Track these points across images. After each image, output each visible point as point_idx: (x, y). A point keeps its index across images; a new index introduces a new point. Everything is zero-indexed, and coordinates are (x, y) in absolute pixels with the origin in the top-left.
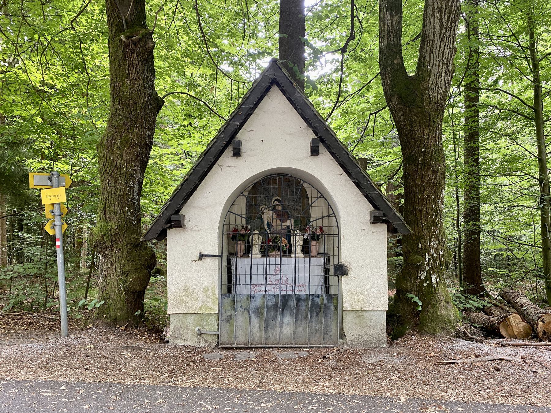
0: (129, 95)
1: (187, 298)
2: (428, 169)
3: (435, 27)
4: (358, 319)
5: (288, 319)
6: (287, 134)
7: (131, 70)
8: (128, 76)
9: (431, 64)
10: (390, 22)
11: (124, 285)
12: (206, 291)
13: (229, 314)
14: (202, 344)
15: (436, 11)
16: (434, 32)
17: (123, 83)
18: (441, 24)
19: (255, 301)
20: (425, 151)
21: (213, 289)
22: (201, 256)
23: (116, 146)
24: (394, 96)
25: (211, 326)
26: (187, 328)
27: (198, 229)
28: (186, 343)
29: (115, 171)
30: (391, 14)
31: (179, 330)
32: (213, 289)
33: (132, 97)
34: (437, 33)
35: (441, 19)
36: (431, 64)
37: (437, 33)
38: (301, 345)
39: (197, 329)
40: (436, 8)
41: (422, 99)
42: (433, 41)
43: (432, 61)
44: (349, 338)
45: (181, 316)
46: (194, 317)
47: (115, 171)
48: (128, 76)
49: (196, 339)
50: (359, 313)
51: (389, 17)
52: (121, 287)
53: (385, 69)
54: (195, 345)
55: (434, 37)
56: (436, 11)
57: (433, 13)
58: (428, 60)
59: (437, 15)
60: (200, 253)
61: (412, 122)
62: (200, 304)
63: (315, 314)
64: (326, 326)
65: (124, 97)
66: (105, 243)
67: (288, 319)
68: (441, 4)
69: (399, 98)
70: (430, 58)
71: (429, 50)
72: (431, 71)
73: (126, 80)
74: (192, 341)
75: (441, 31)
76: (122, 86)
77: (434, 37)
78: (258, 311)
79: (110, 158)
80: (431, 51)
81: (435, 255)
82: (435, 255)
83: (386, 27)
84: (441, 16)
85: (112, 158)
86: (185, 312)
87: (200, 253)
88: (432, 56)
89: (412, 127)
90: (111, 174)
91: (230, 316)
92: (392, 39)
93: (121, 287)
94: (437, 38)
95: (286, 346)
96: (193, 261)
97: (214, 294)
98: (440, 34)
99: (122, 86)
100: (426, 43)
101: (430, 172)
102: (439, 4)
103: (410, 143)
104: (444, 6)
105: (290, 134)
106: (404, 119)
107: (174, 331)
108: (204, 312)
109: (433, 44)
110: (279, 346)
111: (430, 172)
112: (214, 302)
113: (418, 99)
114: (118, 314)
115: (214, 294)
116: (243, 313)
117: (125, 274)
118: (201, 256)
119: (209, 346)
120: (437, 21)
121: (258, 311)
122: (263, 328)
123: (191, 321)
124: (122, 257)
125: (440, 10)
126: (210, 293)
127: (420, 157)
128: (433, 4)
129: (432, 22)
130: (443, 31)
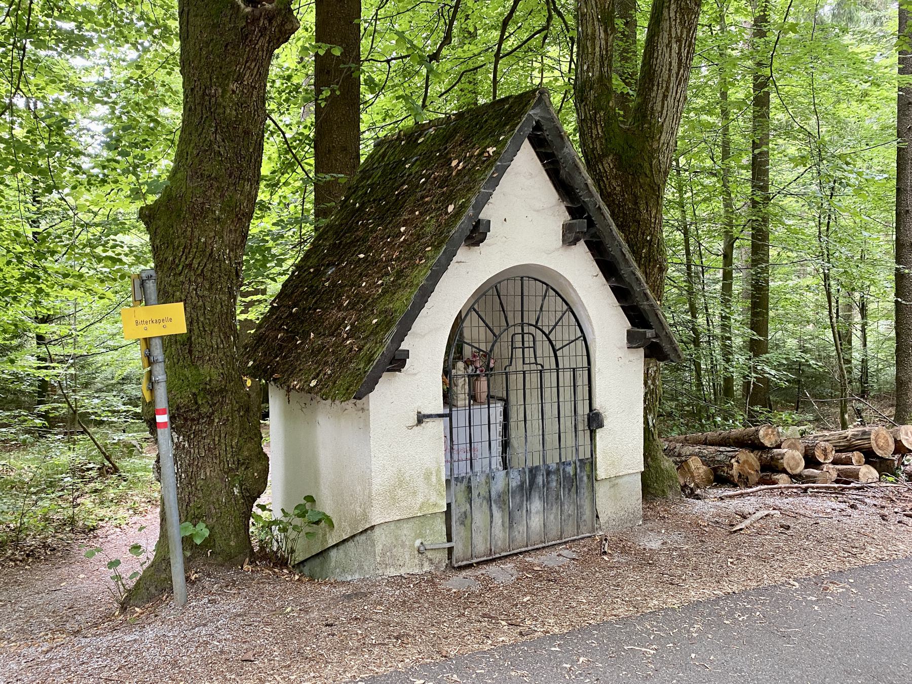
0: (237, 116)
1: (400, 493)
2: (654, 266)
3: (670, 63)
4: (612, 490)
5: (536, 505)
6: (535, 210)
7: (249, 68)
8: (239, 78)
9: (664, 115)
10: (603, 42)
11: (241, 486)
12: (427, 477)
13: (463, 510)
14: (427, 568)
15: (674, 40)
16: (670, 70)
17: (224, 91)
18: (680, 60)
19: (496, 484)
20: (651, 239)
21: (438, 471)
22: (421, 418)
23: (210, 216)
24: (607, 156)
25: (436, 534)
26: (403, 545)
27: (415, 371)
28: (402, 572)
29: (210, 266)
30: (605, 31)
31: (391, 551)
32: (438, 471)
33: (241, 121)
34: (674, 72)
35: (679, 54)
36: (664, 115)
37: (674, 72)
38: (553, 542)
39: (417, 543)
40: (673, 36)
41: (651, 165)
42: (668, 82)
43: (665, 112)
44: (602, 520)
45: (392, 526)
46: (410, 524)
47: (210, 266)
48: (239, 78)
49: (417, 561)
50: (613, 481)
51: (602, 35)
52: (236, 491)
53: (595, 114)
54: (416, 571)
55: (669, 77)
56: (674, 40)
57: (670, 42)
58: (659, 109)
59: (675, 46)
60: (419, 413)
61: (636, 197)
62: (420, 499)
63: (567, 490)
64: (579, 507)
65: (225, 119)
66: (197, 409)
67: (536, 505)
68: (682, 32)
69: (616, 159)
70: (663, 107)
71: (661, 95)
72: (662, 125)
73: (233, 86)
74: (411, 566)
75: (679, 71)
76: (222, 96)
77: (669, 77)
78: (501, 500)
79: (199, 240)
80: (665, 97)
81: (652, 387)
82: (652, 387)
83: (597, 49)
84: (680, 49)
85: (203, 240)
86: (398, 518)
87: (419, 413)
88: (666, 105)
89: (636, 203)
90: (202, 271)
91: (465, 513)
92: (606, 69)
93: (236, 491)
94: (673, 79)
95: (536, 547)
96: (408, 427)
97: (439, 480)
98: (678, 74)
99: (222, 96)
100: (656, 84)
101: (656, 270)
102: (679, 31)
103: (629, 227)
104: (684, 36)
105: (538, 211)
106: (622, 191)
107: (383, 554)
108: (426, 512)
109: (667, 87)
110: (530, 548)
111: (656, 270)
112: (439, 493)
113: (646, 165)
114: (232, 543)
115: (439, 480)
116: (481, 505)
117: (243, 464)
118: (421, 418)
119: (437, 568)
120: (674, 55)
121: (501, 500)
122: (507, 524)
123: (406, 531)
124: (232, 435)
125: (679, 40)
126: (434, 479)
127: (643, 248)
128: (670, 30)
129: (667, 55)
130: (682, 71)
